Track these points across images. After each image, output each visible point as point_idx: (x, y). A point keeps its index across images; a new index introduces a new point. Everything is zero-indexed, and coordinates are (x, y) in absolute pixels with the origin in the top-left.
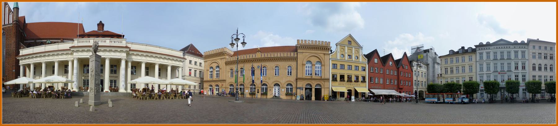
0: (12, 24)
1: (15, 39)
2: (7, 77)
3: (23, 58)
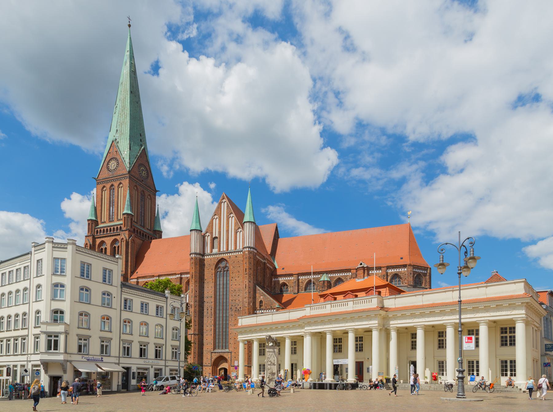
2: (233, 354)
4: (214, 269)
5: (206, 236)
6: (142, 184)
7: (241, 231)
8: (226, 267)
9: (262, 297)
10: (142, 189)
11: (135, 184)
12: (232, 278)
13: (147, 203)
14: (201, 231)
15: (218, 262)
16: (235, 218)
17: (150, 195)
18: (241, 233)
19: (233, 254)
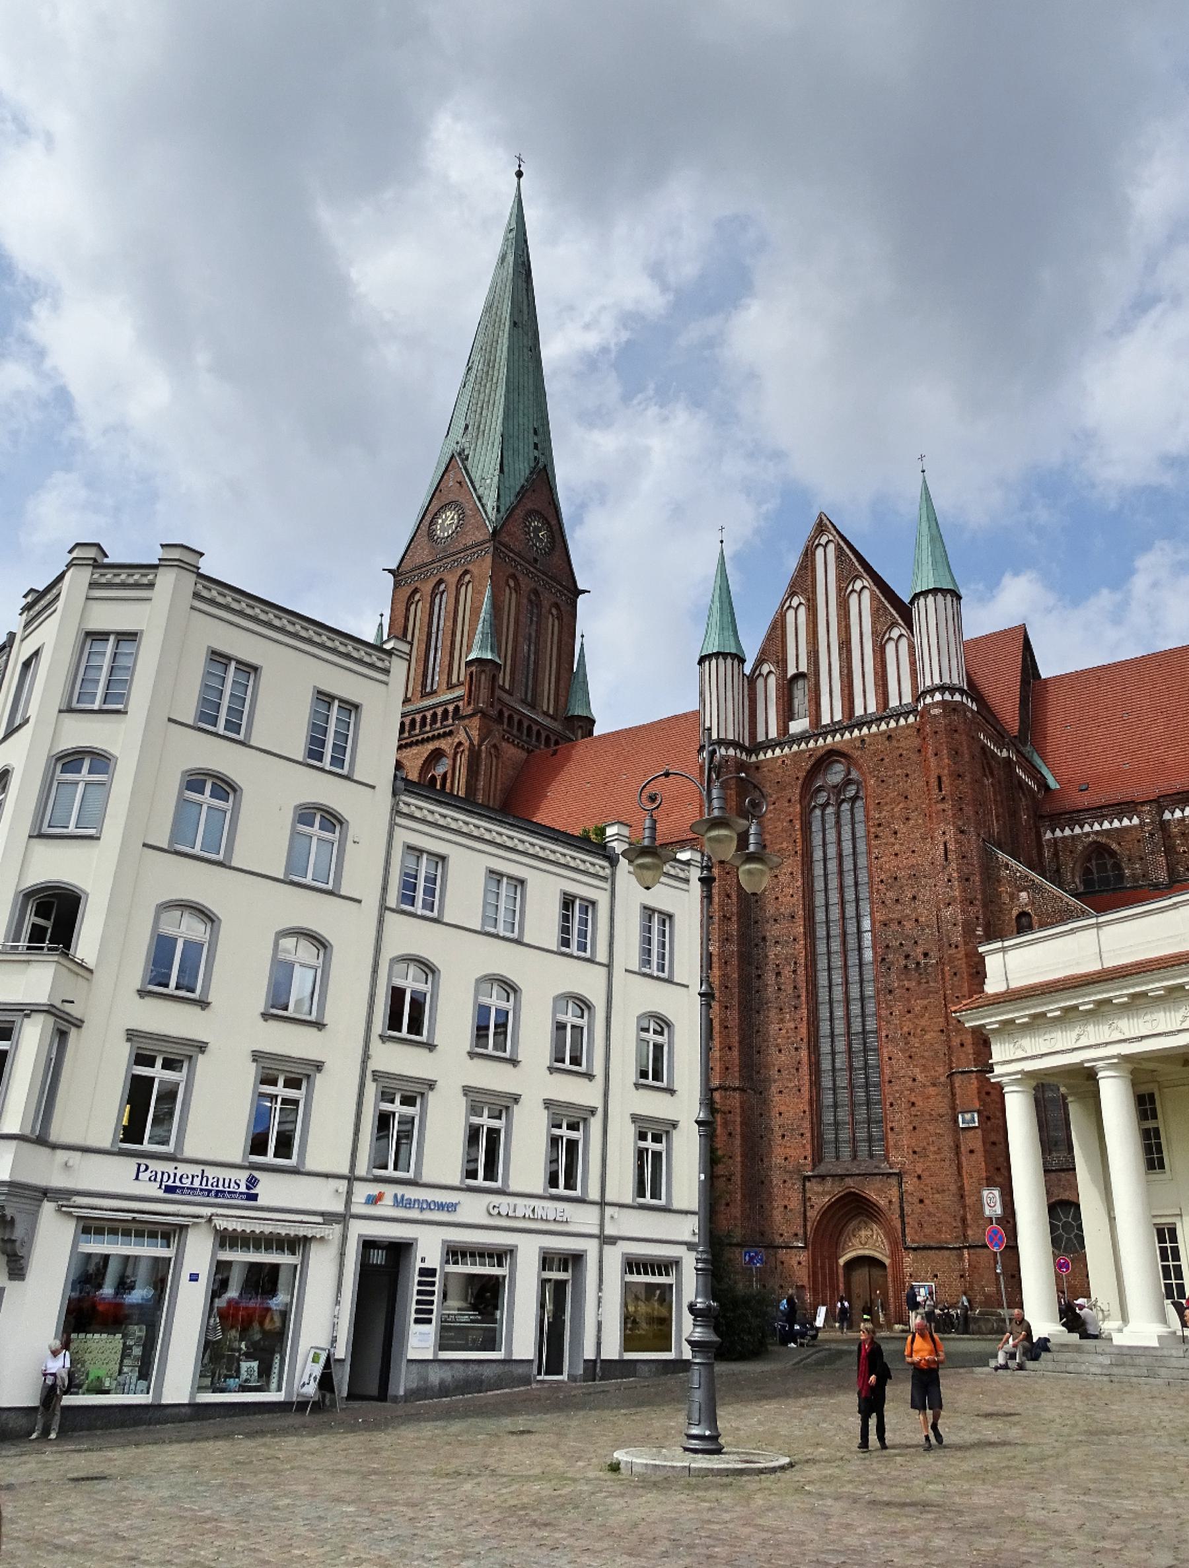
0: (914, 711)
1: (951, 830)
3: (1021, 1015)
4: (798, 798)
5: (760, 674)
6: (532, 569)
7: (901, 636)
8: (848, 782)
9: (1024, 895)
10: (533, 585)
11: (512, 570)
12: (879, 825)
13: (546, 630)
14: (742, 661)
15: (813, 766)
16: (872, 593)
17: (557, 606)
18: (903, 641)
19: (874, 729)
